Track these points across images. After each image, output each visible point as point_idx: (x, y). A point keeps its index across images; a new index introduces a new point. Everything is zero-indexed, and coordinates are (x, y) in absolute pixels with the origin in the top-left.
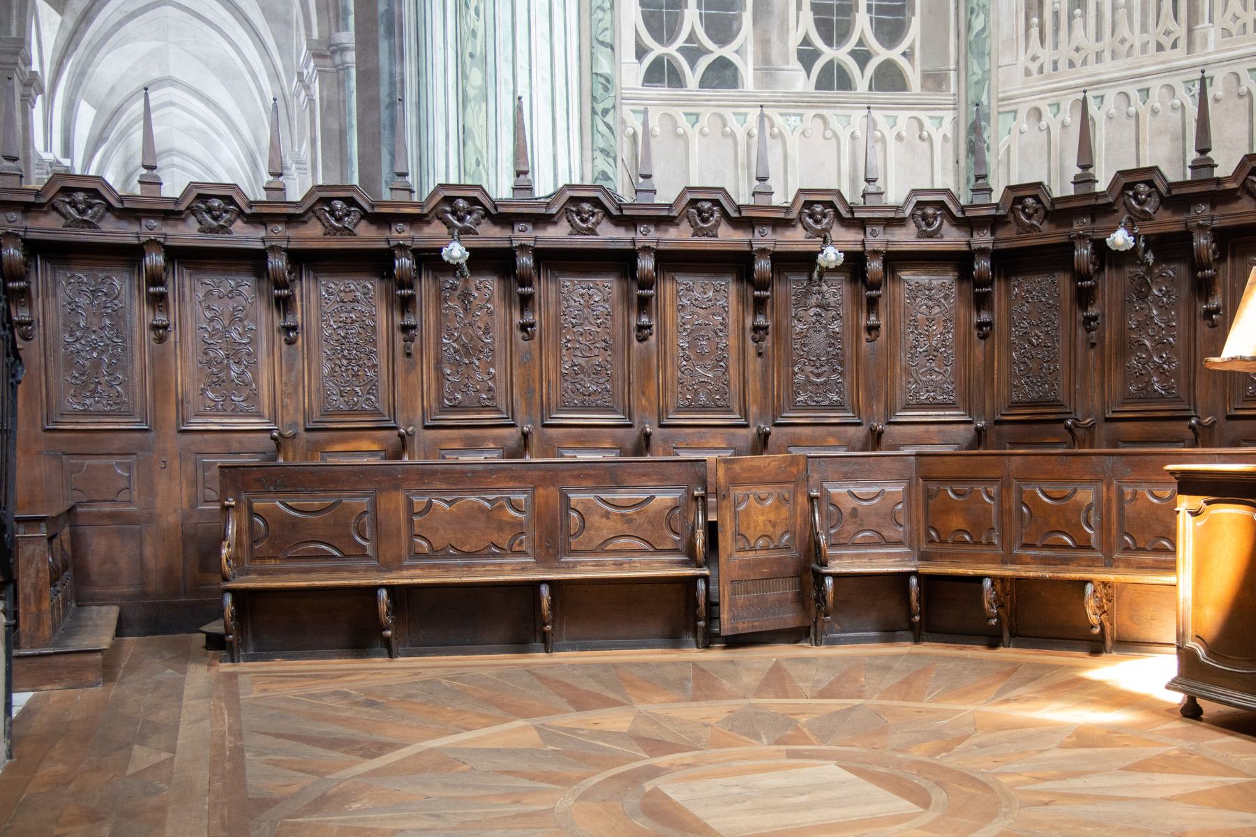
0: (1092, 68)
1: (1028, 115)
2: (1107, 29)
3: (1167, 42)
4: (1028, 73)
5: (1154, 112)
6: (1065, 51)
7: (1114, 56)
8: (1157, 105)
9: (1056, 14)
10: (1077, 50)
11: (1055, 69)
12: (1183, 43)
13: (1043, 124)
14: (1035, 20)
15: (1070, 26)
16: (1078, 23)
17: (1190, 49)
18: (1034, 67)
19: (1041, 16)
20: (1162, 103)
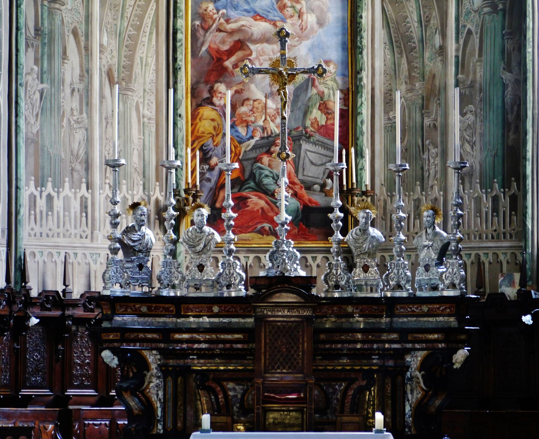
0: (56, 239)
1: (30, 254)
2: (61, 224)
3: (84, 236)
4: (30, 235)
5: (79, 264)
6: (45, 230)
7: (64, 236)
8: (80, 261)
9: (41, 212)
10: (50, 230)
11: (41, 236)
12: (89, 237)
13: (36, 259)
14: (33, 212)
15: (47, 219)
16: (50, 218)
17: (92, 240)
18: (32, 233)
19: (35, 211)
20: (82, 260)
